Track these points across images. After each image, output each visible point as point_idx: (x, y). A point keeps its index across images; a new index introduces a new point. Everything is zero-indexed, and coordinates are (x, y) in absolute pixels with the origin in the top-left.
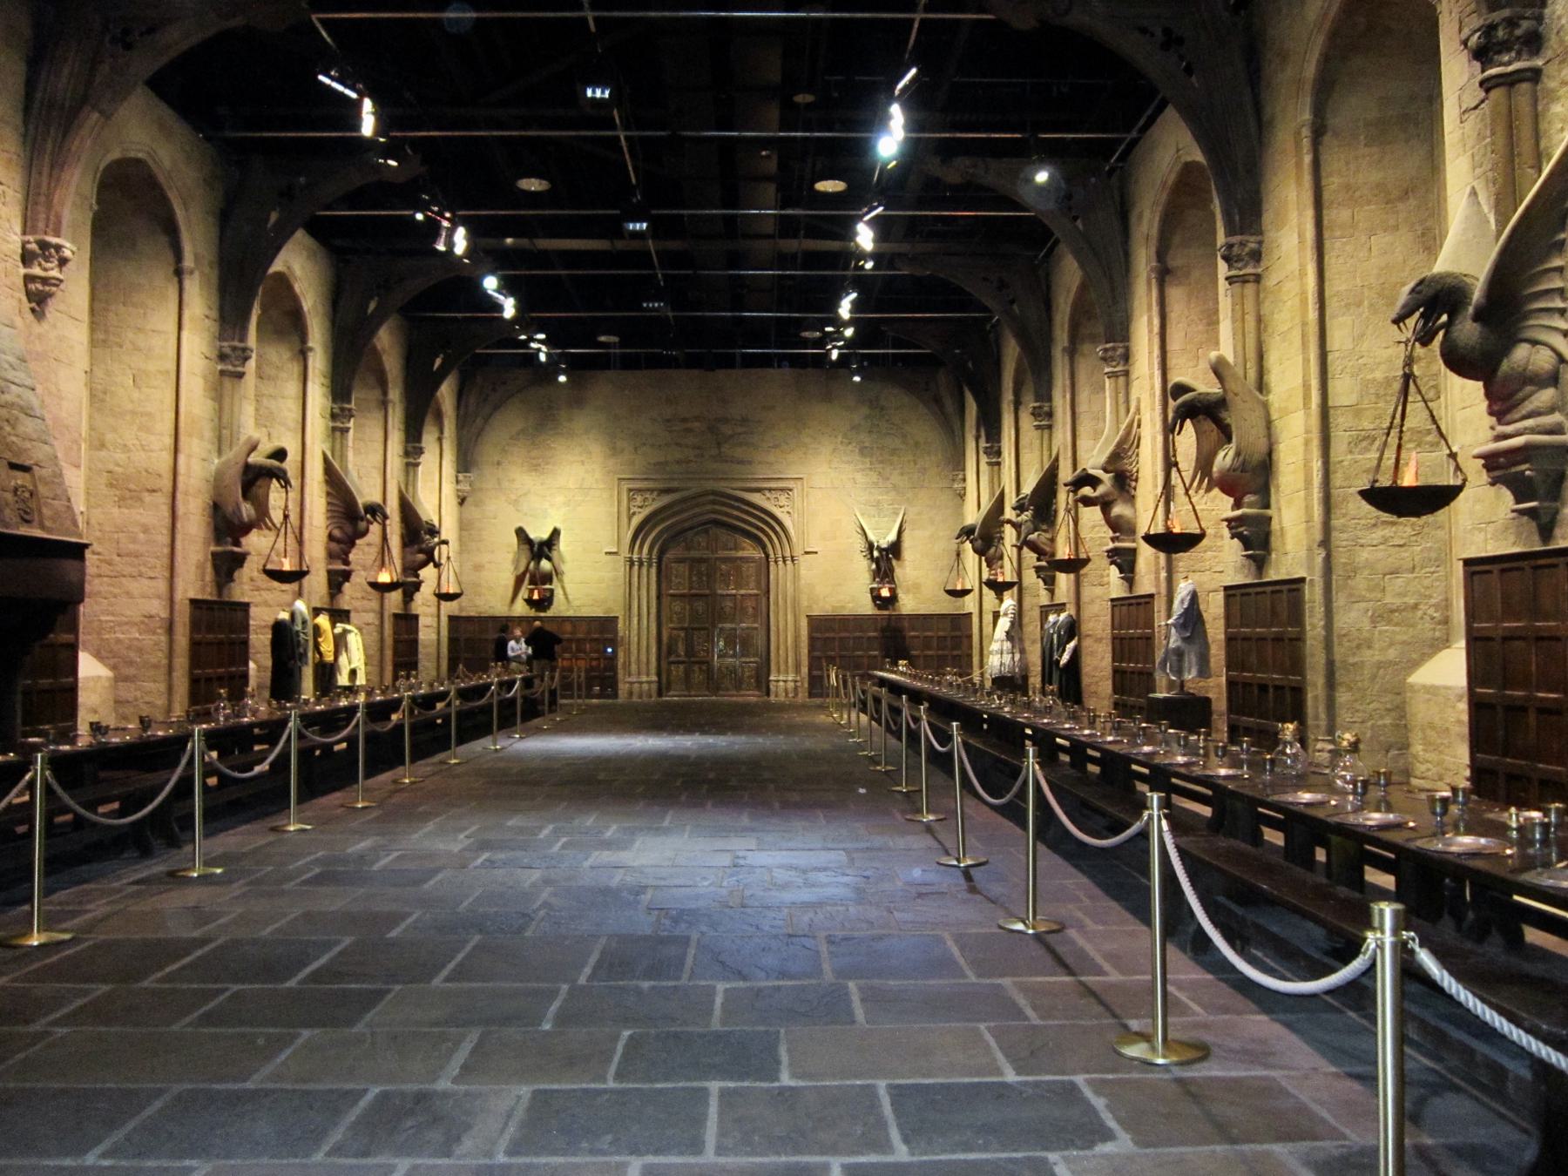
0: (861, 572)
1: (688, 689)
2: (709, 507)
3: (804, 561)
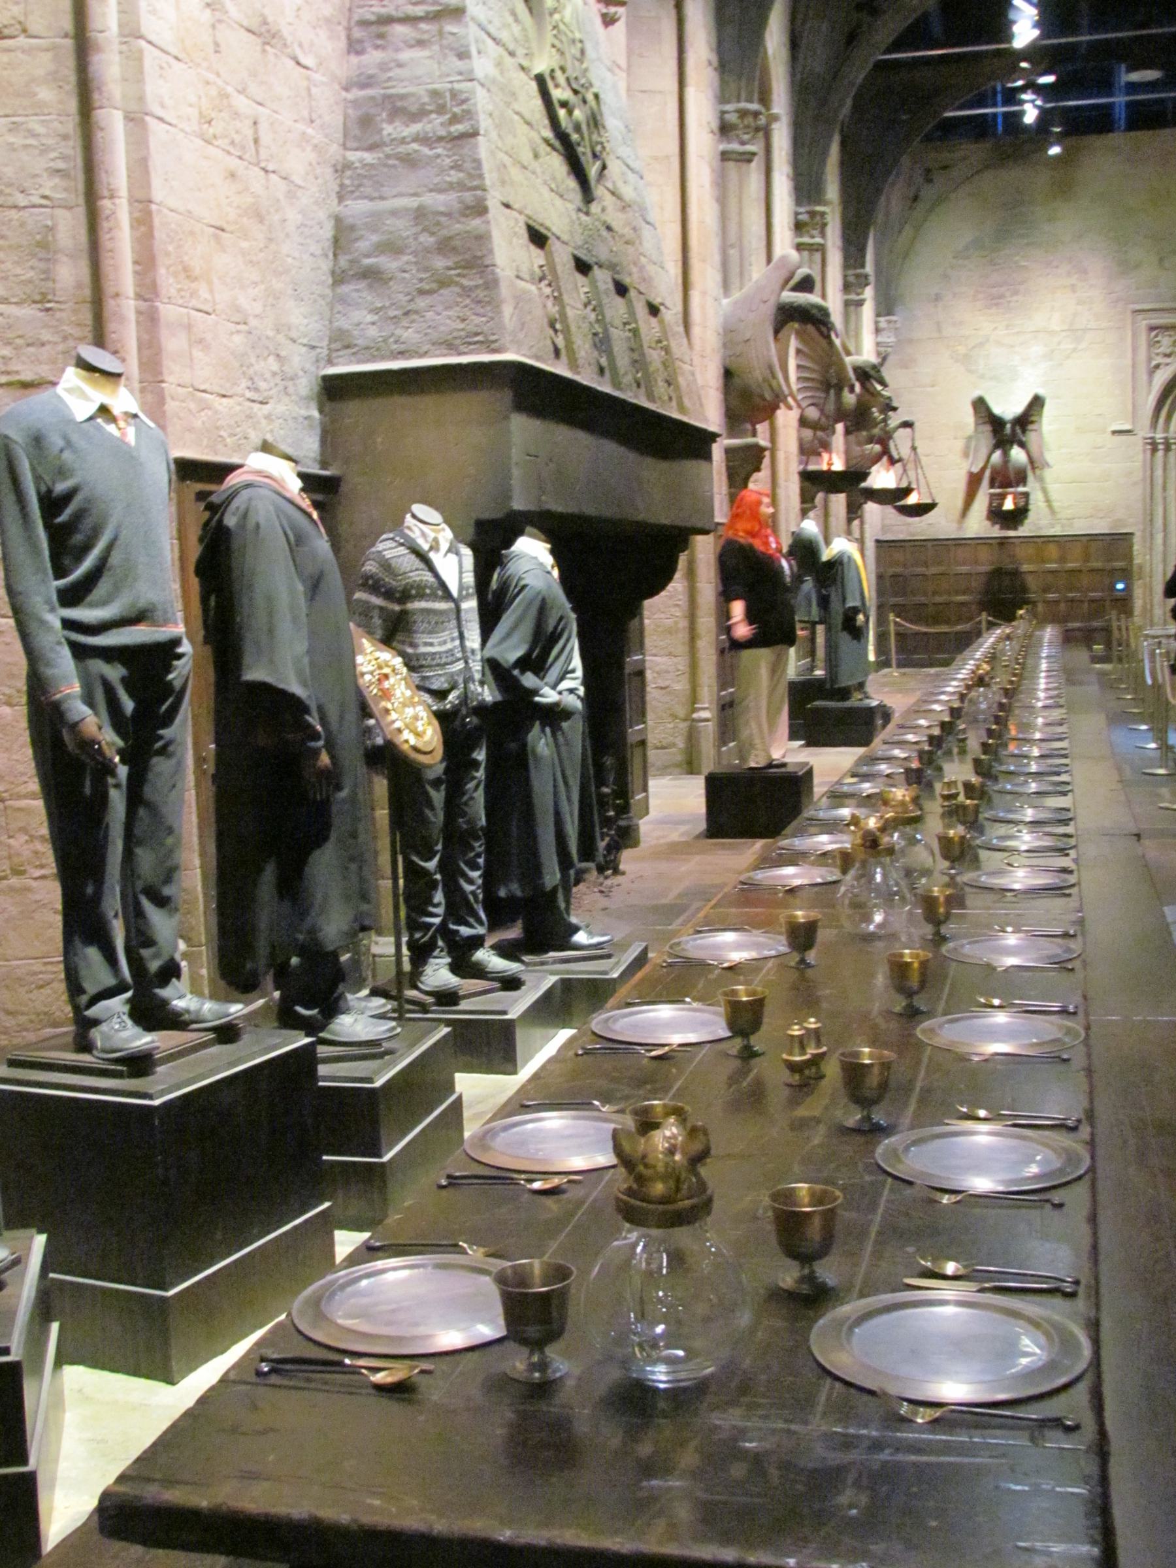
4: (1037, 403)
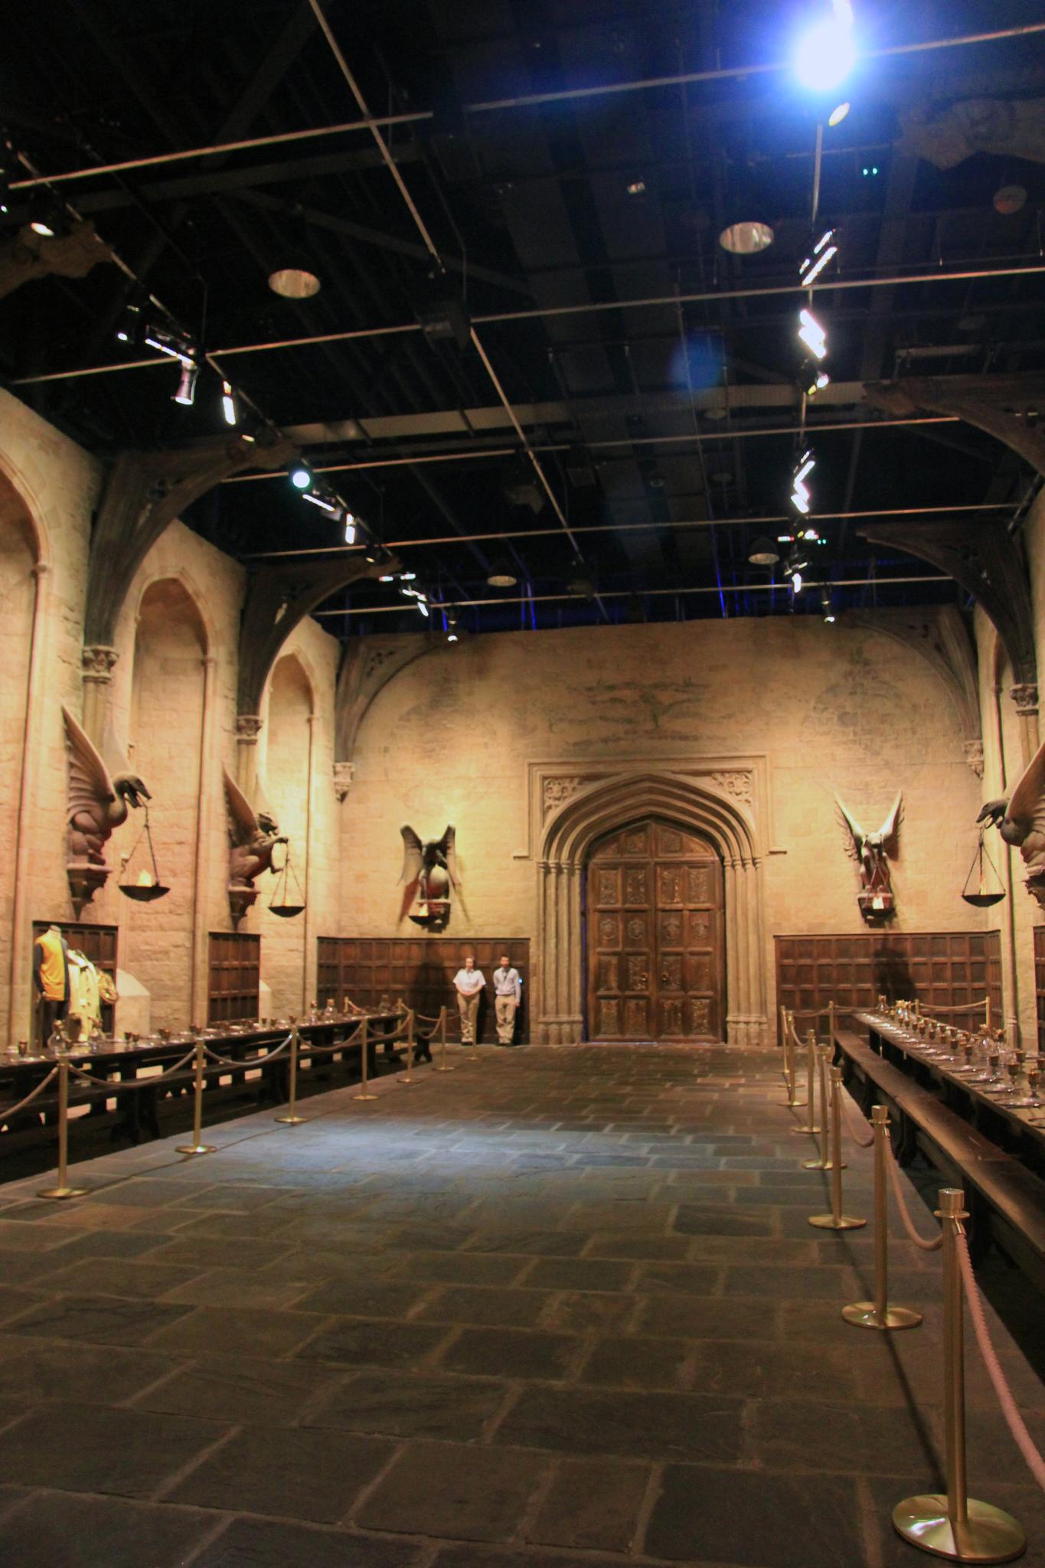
0: (848, 873)
1: (622, 1031)
2: (645, 797)
3: (768, 864)
4: (450, 832)
